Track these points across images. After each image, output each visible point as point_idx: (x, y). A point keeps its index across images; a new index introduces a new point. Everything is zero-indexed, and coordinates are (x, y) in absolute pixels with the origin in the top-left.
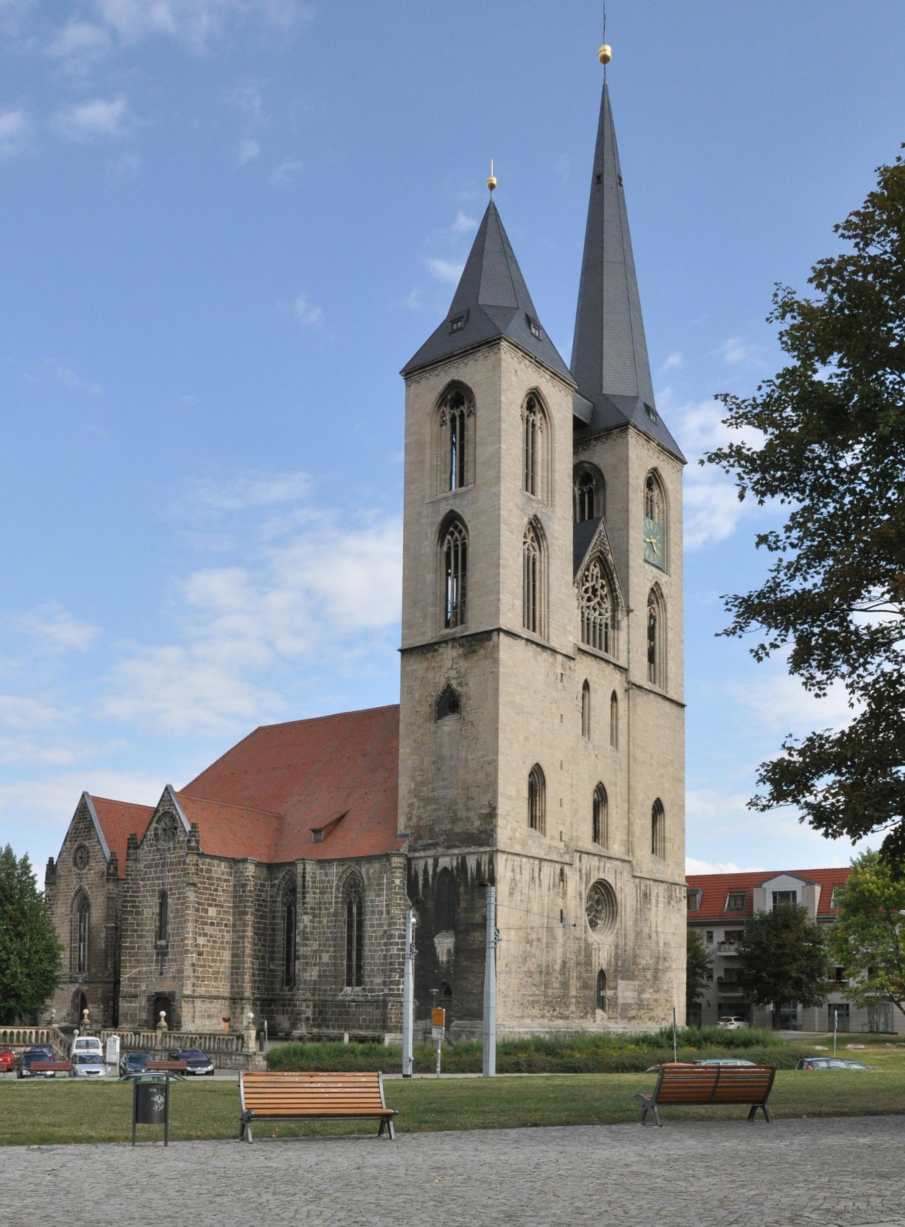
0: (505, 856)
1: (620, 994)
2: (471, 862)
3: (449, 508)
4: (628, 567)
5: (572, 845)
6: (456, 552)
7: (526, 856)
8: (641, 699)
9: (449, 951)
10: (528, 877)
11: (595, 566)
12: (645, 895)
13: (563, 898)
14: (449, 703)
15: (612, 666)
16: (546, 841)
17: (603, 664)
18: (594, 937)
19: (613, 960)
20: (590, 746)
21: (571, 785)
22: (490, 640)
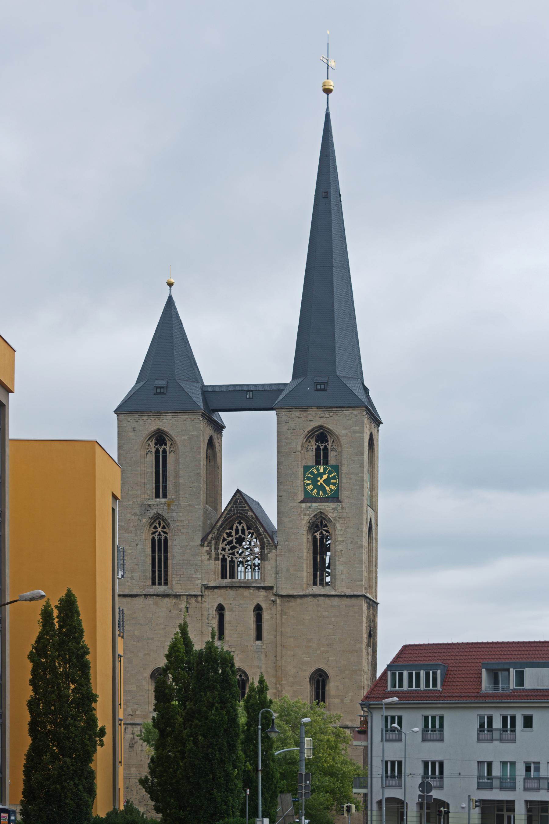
11: (240, 523)
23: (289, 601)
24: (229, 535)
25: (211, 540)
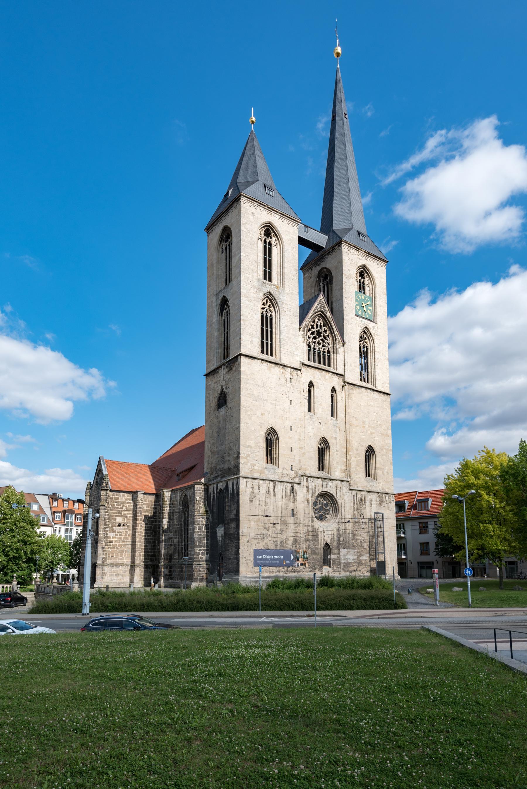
0: (245, 480)
1: (342, 557)
2: (230, 485)
3: (223, 295)
4: (343, 319)
5: (301, 473)
7: (263, 480)
8: (356, 391)
9: (222, 535)
10: (264, 492)
12: (361, 500)
13: (293, 503)
15: (331, 373)
16: (280, 471)
17: (324, 372)
18: (319, 525)
19: (336, 537)
20: (315, 418)
21: (299, 439)
22: (237, 361)
23: (352, 389)
24: (312, 326)
25: (305, 327)
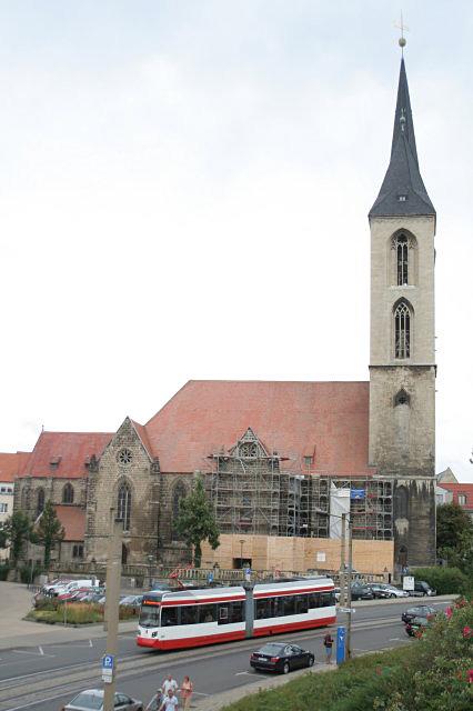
6: (402, 319)
14: (402, 398)
